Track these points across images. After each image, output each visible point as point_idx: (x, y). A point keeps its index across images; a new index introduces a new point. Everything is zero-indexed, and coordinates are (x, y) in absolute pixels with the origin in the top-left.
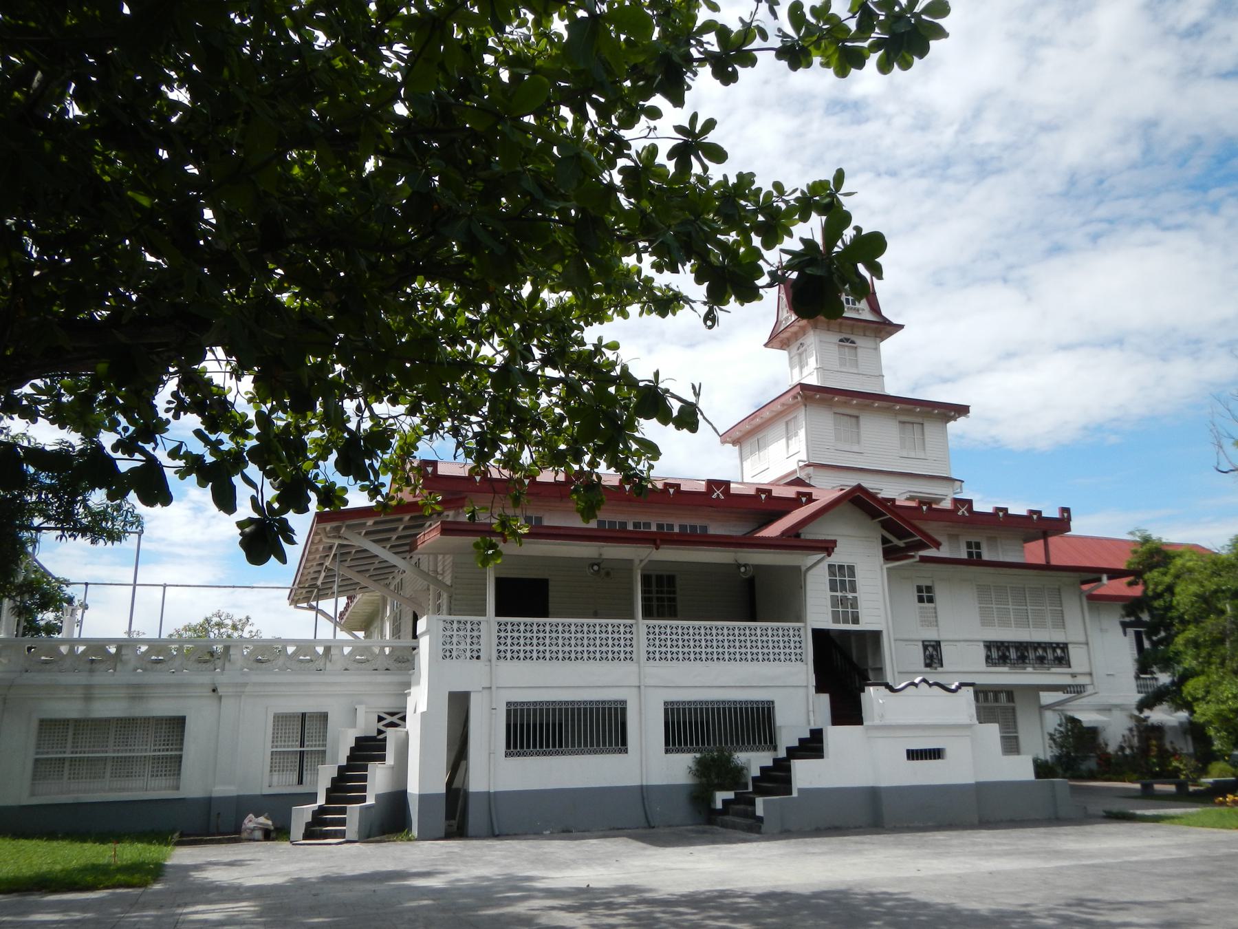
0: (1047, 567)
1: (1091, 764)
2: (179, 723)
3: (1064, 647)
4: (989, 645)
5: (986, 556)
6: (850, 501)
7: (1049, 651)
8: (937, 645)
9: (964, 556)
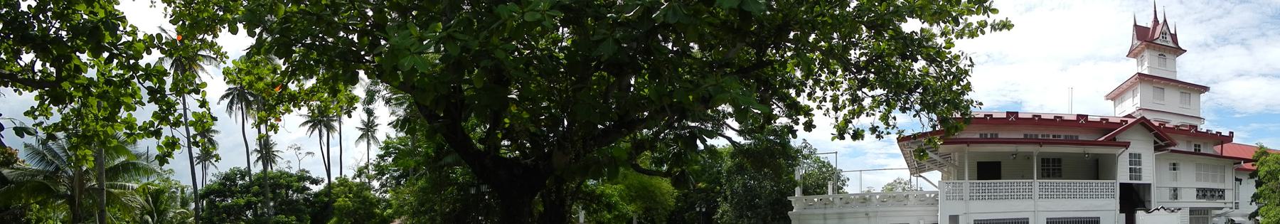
4: (1198, 190)
5: (1202, 151)
8: (1175, 190)
9: (1193, 151)
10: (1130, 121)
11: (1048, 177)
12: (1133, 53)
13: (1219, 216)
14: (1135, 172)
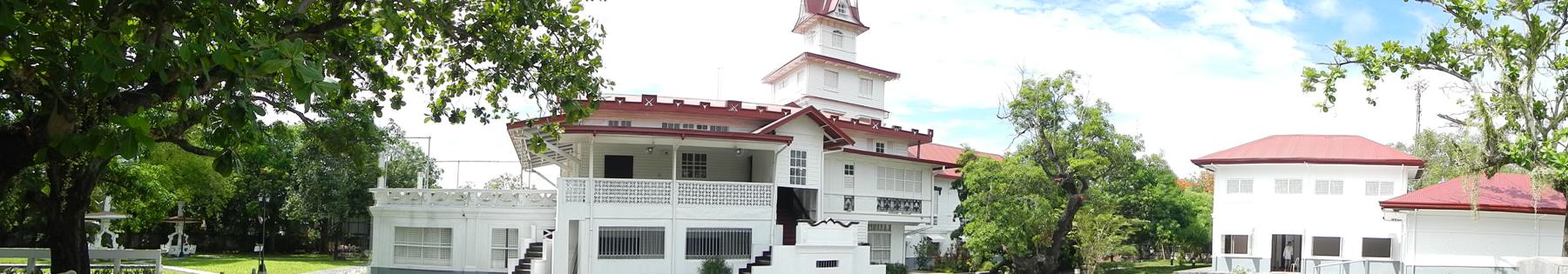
1: (932, 263)
2: (449, 231)
3: (919, 202)
4: (880, 200)
6: (807, 114)
7: (912, 204)
8: (852, 198)
10: (794, 111)
11: (690, 176)
12: (800, 28)
13: (913, 232)
14: (797, 173)
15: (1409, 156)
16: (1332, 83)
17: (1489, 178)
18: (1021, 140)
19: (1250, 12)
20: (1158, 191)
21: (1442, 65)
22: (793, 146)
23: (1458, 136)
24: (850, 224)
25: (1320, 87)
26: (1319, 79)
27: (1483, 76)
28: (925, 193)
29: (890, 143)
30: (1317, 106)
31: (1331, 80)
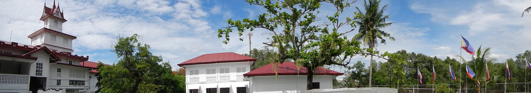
0: (83, 67)
3: (84, 82)
5: (72, 64)
7: (81, 82)
10: (38, 48)
12: (43, 19)
14: (39, 72)
15: (251, 58)
16: (228, 34)
17: (281, 64)
18: (119, 59)
19: (192, 14)
20: (167, 75)
21: (263, 26)
22: (39, 61)
23: (265, 51)
24: (59, 90)
25: (224, 35)
26: (223, 33)
27: (277, 29)
28: (86, 78)
29: (74, 61)
30: (223, 42)
31: (227, 33)
